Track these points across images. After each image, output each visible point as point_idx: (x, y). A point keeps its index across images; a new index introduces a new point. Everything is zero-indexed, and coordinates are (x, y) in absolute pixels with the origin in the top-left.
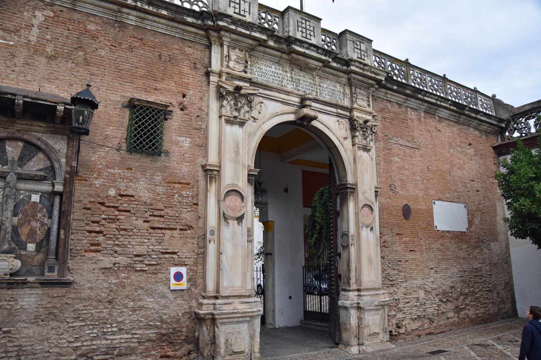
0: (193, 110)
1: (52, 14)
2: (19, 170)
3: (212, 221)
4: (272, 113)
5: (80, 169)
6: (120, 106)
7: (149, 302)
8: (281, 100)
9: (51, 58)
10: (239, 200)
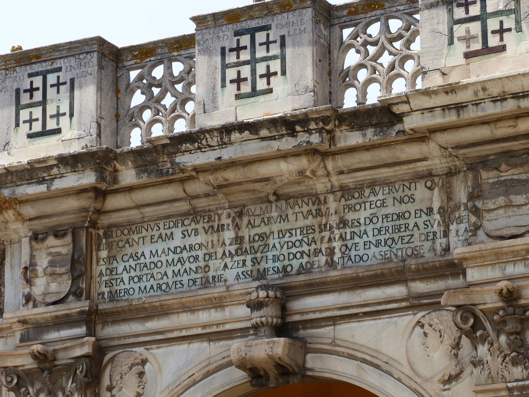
8: (200, 331)
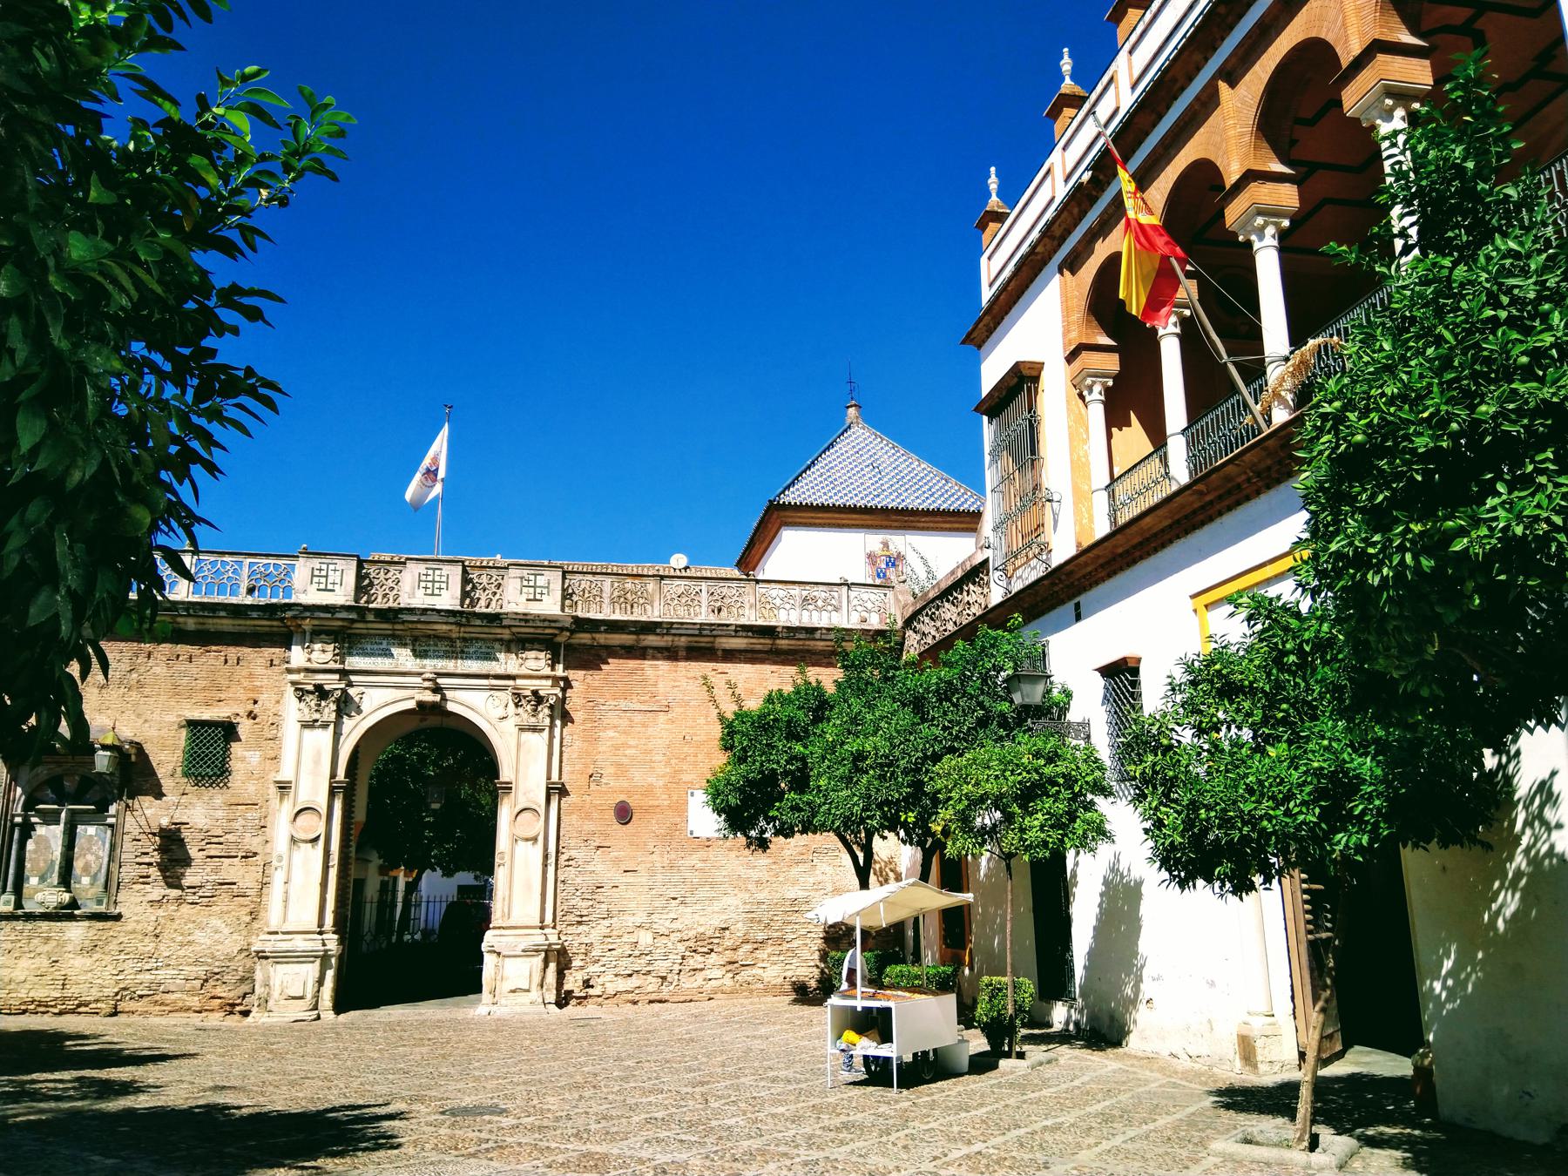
3: (281, 843)
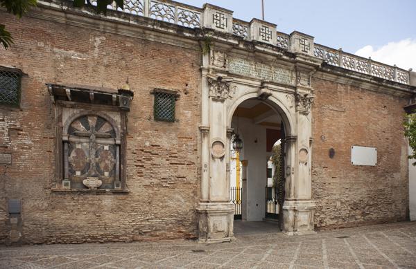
0: (193, 94)
1: (105, 39)
2: (97, 133)
4: (242, 93)
5: (128, 131)
6: (149, 93)
7: (170, 203)
9: (107, 66)
10: (221, 147)
